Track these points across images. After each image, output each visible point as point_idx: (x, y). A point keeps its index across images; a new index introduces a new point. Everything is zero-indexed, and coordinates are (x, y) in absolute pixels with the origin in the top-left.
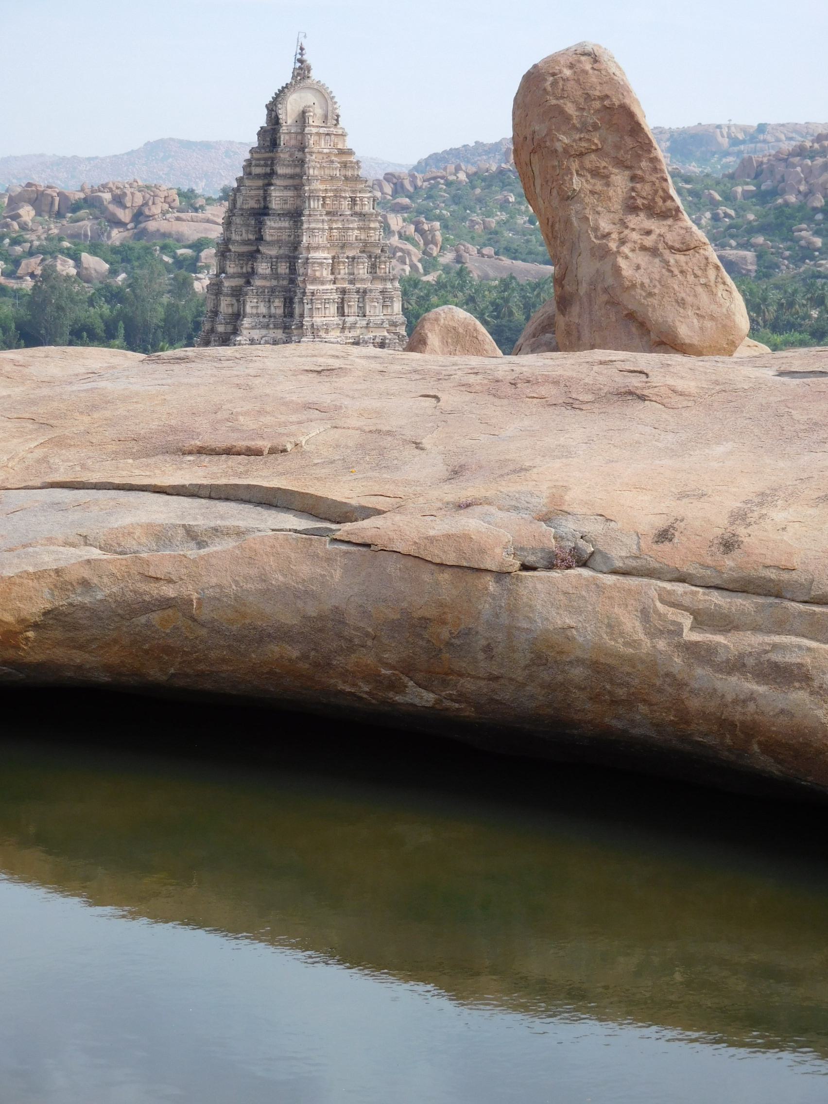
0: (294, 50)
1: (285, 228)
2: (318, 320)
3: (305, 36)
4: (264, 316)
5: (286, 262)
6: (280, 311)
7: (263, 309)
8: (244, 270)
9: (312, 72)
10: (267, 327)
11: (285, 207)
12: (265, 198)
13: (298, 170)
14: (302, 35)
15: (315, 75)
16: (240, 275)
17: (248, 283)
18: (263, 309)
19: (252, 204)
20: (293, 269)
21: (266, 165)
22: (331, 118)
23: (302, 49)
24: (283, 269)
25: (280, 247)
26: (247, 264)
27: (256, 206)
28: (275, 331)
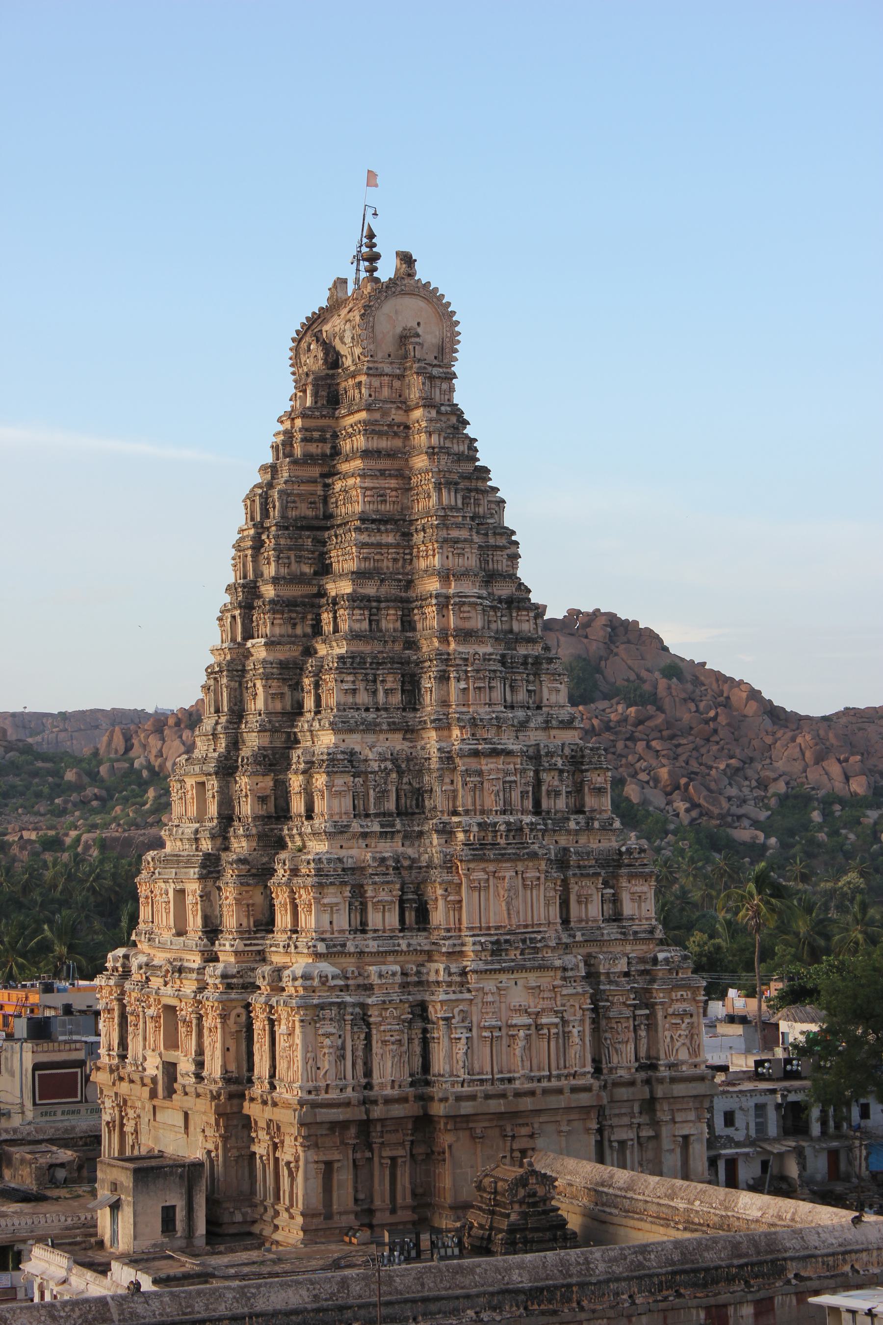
0: (351, 242)
1: (388, 546)
2: (483, 711)
3: (375, 214)
4: (367, 710)
5: (396, 608)
6: (396, 699)
7: (363, 698)
8: (299, 631)
9: (417, 265)
10: (371, 728)
11: (382, 507)
12: (325, 500)
13: (398, 443)
14: (370, 212)
15: (422, 273)
16: (292, 639)
17: (309, 652)
18: (363, 698)
19: (304, 510)
20: (408, 624)
21: (323, 440)
22: (446, 350)
23: (371, 235)
24: (390, 622)
25: (382, 581)
26: (304, 618)
27: (310, 513)
28: (389, 736)
